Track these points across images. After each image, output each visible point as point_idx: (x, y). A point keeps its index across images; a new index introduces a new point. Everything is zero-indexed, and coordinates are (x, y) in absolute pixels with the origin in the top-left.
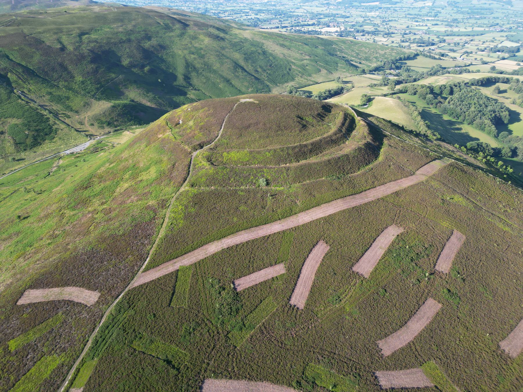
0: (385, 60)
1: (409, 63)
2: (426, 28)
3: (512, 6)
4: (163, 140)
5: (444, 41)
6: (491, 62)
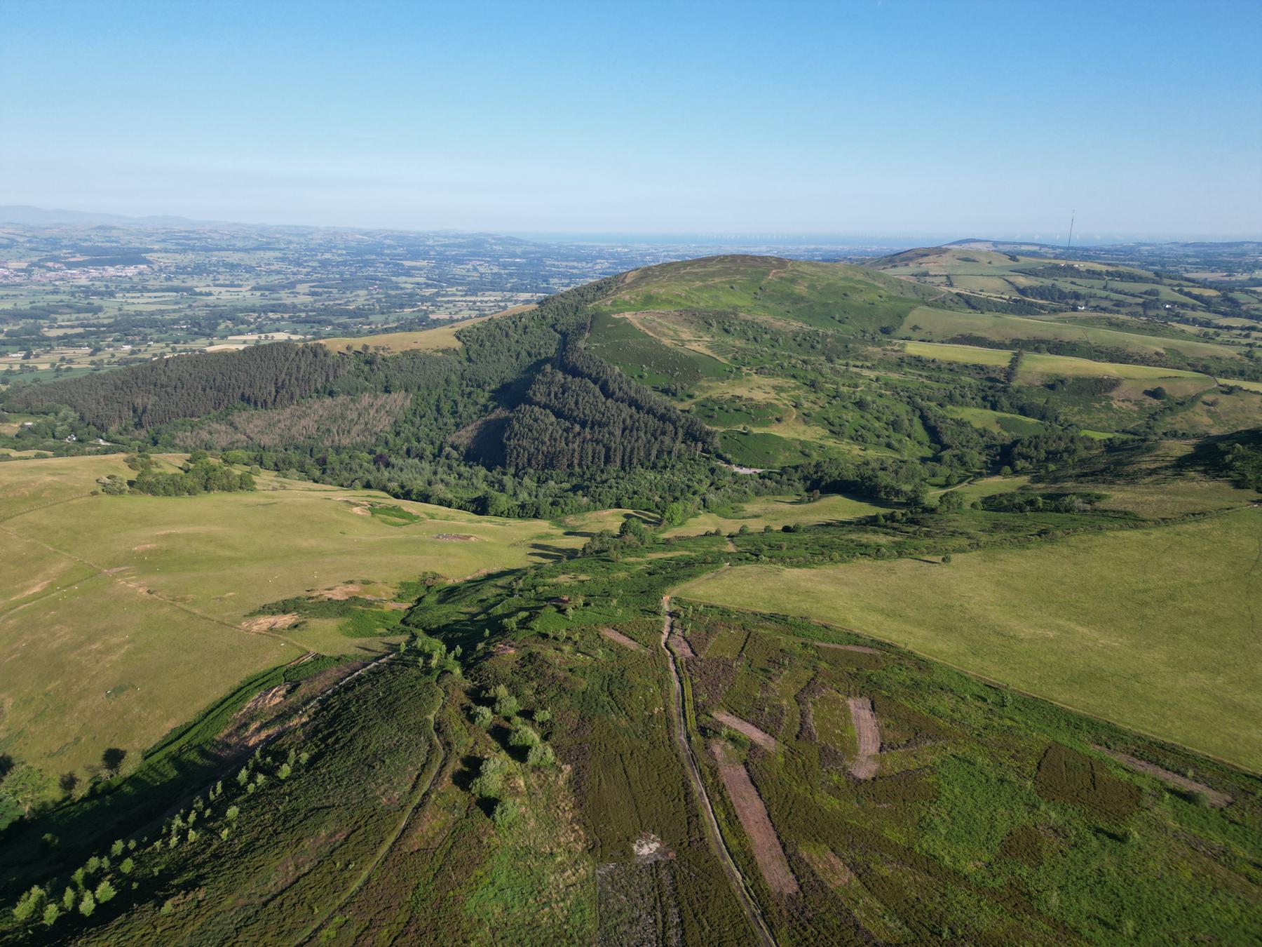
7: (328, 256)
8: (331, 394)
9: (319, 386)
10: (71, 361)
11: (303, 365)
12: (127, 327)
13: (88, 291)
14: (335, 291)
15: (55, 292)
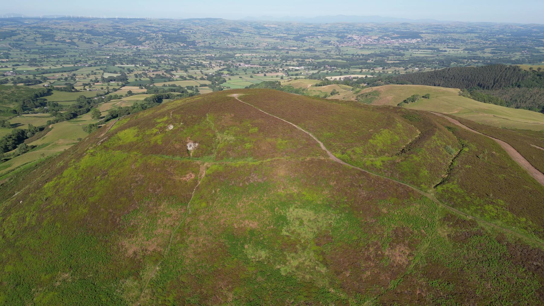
0: (21, 99)
1: (49, 98)
2: (11, 69)
3: (78, 46)
5: (45, 79)
6: (119, 89)
7: (501, 36)
8: (519, 86)
9: (514, 82)
10: (398, 71)
11: (508, 75)
12: (415, 62)
13: (399, 48)
15: (387, 48)
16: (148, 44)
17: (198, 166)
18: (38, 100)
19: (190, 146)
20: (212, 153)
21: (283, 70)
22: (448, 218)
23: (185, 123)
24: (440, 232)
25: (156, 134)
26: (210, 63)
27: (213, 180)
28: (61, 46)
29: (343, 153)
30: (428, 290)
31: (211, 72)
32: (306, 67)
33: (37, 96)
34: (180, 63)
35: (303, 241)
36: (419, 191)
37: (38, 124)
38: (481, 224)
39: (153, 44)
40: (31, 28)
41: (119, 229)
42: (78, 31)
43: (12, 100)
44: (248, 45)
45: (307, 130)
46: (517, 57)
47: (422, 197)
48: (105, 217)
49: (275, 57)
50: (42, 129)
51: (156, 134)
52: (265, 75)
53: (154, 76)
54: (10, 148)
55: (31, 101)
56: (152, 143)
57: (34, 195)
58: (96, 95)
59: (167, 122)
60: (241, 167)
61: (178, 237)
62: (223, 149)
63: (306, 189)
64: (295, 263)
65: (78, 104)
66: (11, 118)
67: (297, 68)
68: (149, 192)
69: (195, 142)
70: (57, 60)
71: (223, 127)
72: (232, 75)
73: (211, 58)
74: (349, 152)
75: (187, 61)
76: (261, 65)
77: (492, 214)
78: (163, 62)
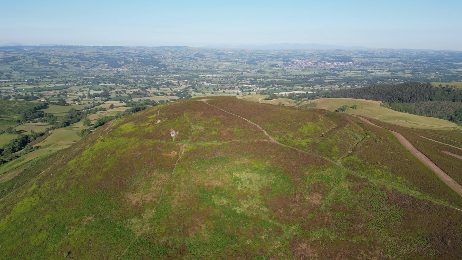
0: (23, 111)
1: (46, 111)
2: (13, 88)
3: (68, 69)
4: (191, 153)
5: (41, 96)
6: (102, 103)
7: (418, 60)
8: (431, 100)
9: (427, 97)
10: (334, 88)
12: (348, 81)
13: (334, 70)
14: (421, 73)
15: (325, 70)
16: (127, 67)
17: (179, 146)
18: (37, 112)
19: (173, 134)
20: (188, 138)
21: (239, 87)
22: (349, 177)
23: (169, 118)
24: (343, 185)
25: (148, 126)
26: (178, 82)
27: (190, 155)
28: (54, 69)
29: (280, 138)
30: (333, 219)
31: (179, 89)
32: (258, 85)
33: (36, 109)
34: (153, 82)
35: (252, 193)
36: (331, 161)
37: (38, 130)
38: (371, 180)
39: (131, 67)
40: (29, 54)
41: (125, 188)
42: (68, 57)
43: (16, 112)
44: (210, 67)
45: (255, 123)
46: (432, 77)
47: (332, 164)
48: (115, 181)
49: (232, 77)
50: (42, 135)
51: (148, 126)
52: (224, 92)
53: (131, 93)
54: (17, 149)
55: (31, 113)
56: (146, 132)
57: (61, 169)
58: (84, 108)
59: (156, 118)
60: (208, 147)
61: (167, 192)
62: (196, 135)
63: (254, 161)
64: (247, 206)
65: (70, 116)
66: (16, 126)
67: (250, 86)
68: (145, 164)
69: (176, 131)
70: (51, 80)
71: (196, 121)
72: (197, 92)
73: (179, 78)
74: (284, 136)
75: (159, 81)
76: (220, 84)
77: (379, 174)
78: (139, 81)
